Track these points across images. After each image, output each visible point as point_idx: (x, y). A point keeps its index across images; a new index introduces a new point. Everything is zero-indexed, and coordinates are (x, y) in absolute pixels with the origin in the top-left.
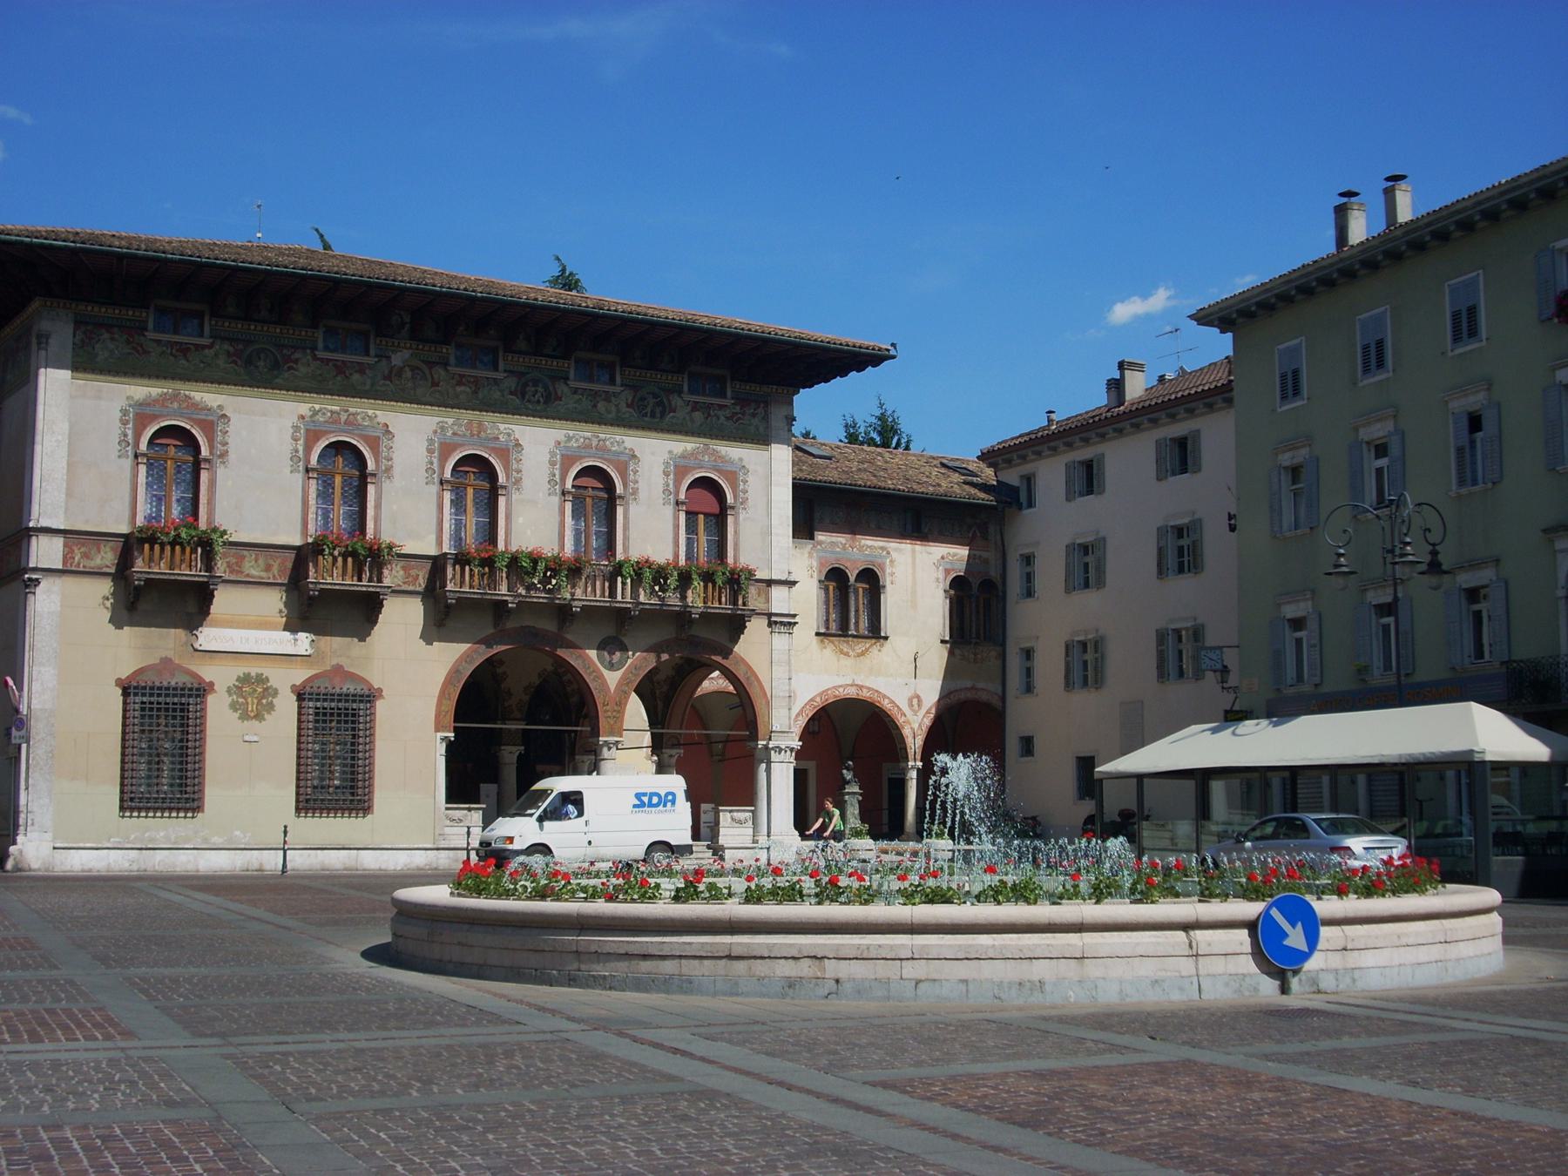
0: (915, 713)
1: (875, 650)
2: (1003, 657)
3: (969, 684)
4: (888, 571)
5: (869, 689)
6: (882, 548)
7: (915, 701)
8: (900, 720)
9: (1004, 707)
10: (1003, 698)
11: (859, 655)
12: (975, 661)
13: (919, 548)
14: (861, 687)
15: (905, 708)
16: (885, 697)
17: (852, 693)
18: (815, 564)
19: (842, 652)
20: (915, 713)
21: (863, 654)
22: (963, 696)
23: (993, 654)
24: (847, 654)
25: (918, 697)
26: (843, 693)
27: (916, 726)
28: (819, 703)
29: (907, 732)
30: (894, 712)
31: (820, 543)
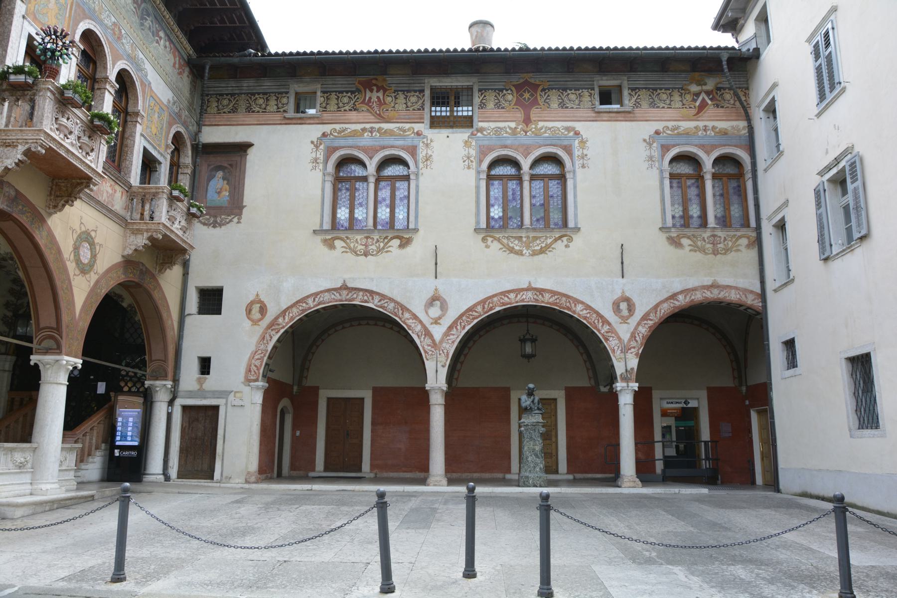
0: (624, 320)
1: (560, 245)
2: (758, 242)
3: (708, 281)
4: (577, 152)
5: (554, 293)
6: (568, 129)
7: (623, 306)
8: (601, 331)
9: (765, 306)
10: (763, 296)
11: (535, 254)
12: (715, 253)
13: (623, 128)
14: (541, 291)
15: (608, 313)
16: (577, 301)
17: (528, 299)
18: (473, 152)
19: (512, 250)
20: (624, 320)
21: (542, 251)
22: (698, 297)
23: (744, 242)
24: (520, 253)
25: (628, 300)
26: (514, 300)
27: (626, 337)
28: (481, 314)
29: (611, 345)
30: (589, 320)
31: (481, 130)
